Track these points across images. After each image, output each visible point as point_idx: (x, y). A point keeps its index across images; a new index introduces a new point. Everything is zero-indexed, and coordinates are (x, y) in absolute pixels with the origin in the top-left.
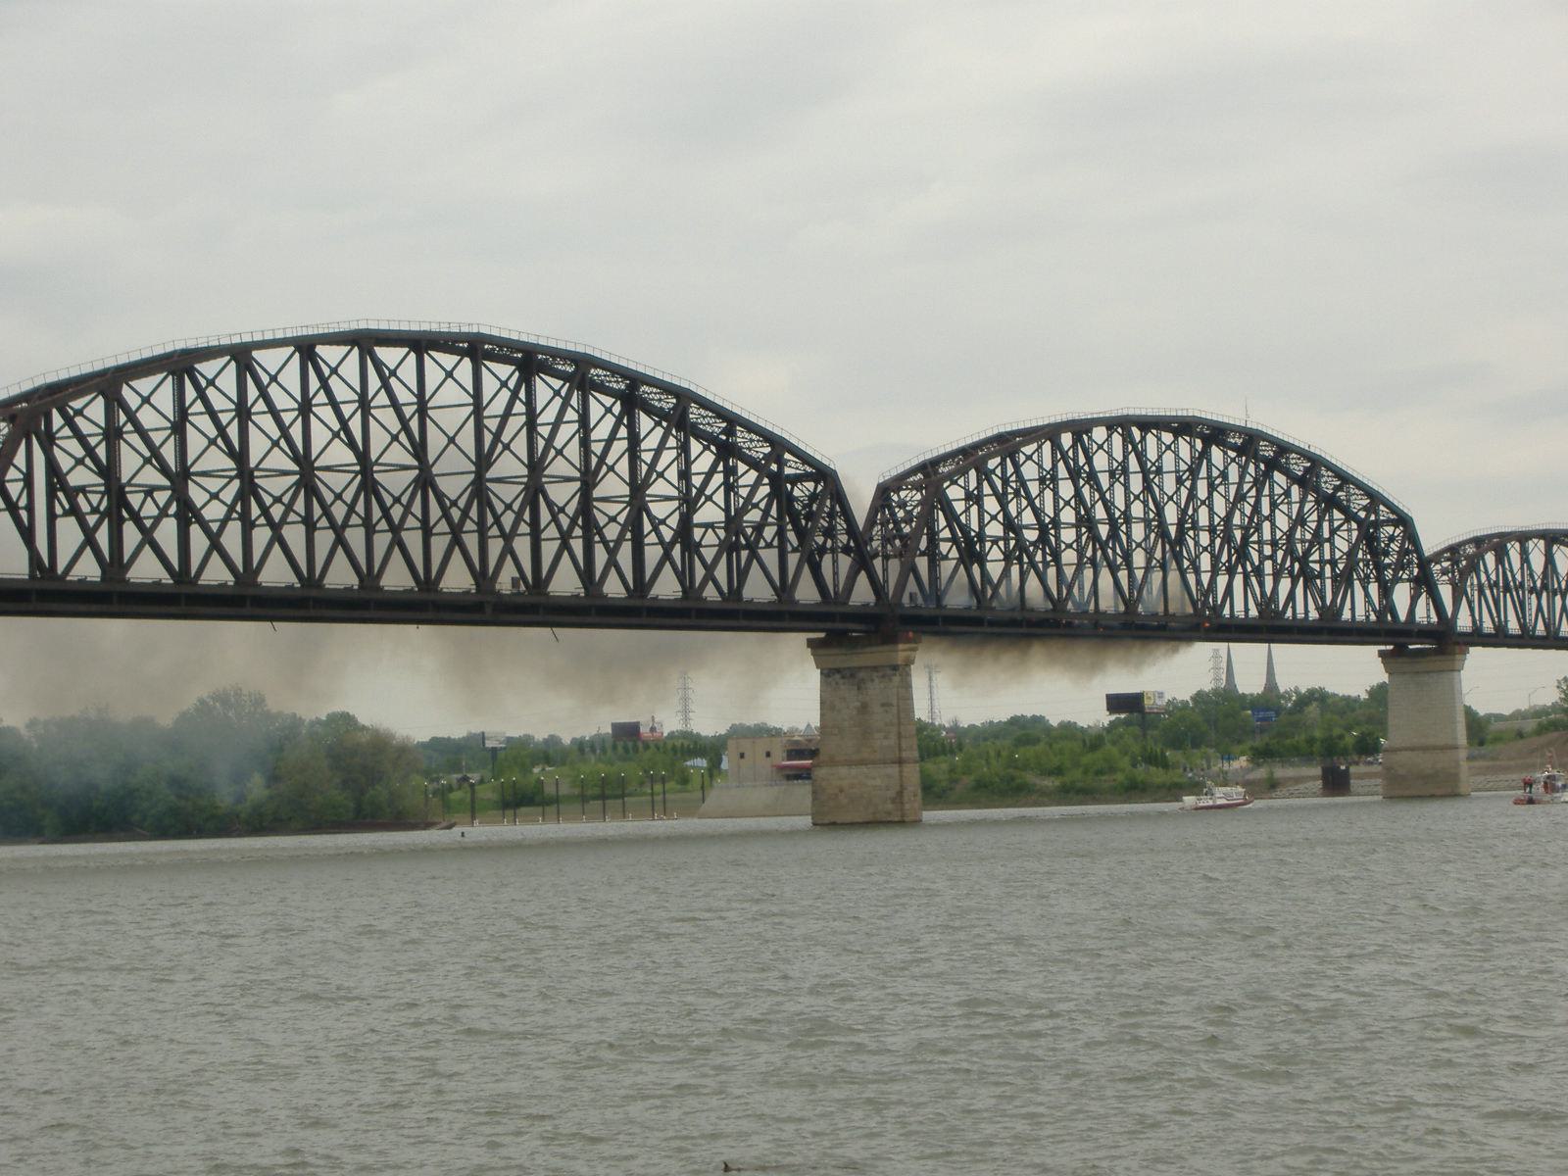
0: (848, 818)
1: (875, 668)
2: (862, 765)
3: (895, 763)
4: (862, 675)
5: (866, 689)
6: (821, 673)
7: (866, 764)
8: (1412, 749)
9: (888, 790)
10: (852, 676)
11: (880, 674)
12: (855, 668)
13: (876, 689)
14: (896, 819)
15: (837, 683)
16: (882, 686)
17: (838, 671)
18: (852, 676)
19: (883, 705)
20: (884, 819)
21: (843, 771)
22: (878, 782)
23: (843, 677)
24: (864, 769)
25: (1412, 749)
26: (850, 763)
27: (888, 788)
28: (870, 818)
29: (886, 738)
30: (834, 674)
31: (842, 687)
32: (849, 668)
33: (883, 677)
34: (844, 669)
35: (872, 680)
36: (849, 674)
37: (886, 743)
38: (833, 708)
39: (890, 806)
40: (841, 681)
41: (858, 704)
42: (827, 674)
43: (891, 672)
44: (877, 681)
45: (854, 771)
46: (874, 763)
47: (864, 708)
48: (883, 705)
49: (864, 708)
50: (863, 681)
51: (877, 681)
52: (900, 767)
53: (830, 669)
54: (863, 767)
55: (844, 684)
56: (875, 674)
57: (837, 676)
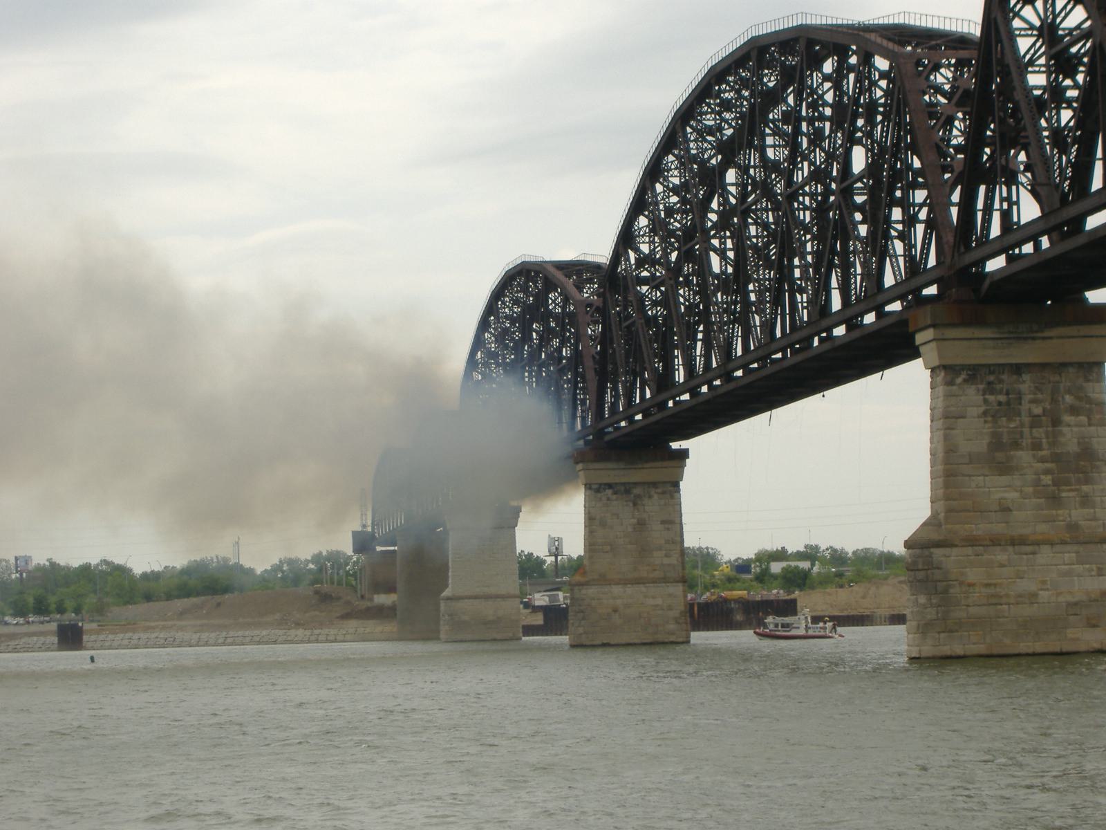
0: (625, 640)
1: (654, 484)
2: (639, 583)
3: (677, 582)
4: (637, 491)
5: (643, 505)
6: (585, 487)
7: (644, 583)
8: (476, 597)
9: (671, 610)
10: (628, 492)
11: (659, 490)
12: (629, 483)
13: (653, 506)
14: (681, 640)
15: (608, 499)
16: (662, 502)
17: (610, 486)
18: (628, 492)
19: (663, 522)
20: (666, 640)
21: (617, 590)
22: (659, 601)
23: (615, 493)
24: (642, 588)
25: (476, 597)
26: (625, 582)
27: (670, 608)
28: (649, 639)
29: (666, 556)
30: (605, 489)
31: (615, 503)
32: (624, 484)
33: (664, 493)
34: (616, 484)
35: (650, 497)
36: (624, 490)
37: (666, 561)
38: (603, 524)
39: (672, 626)
40: (614, 497)
41: (635, 521)
42: (595, 490)
43: (672, 488)
44: (656, 497)
45: (630, 590)
46: (654, 581)
47: (641, 524)
48: (663, 522)
49: (641, 524)
50: (638, 496)
51: (656, 497)
52: (684, 586)
53: (601, 484)
54: (642, 585)
55: (616, 500)
56: (653, 491)
57: (609, 492)
